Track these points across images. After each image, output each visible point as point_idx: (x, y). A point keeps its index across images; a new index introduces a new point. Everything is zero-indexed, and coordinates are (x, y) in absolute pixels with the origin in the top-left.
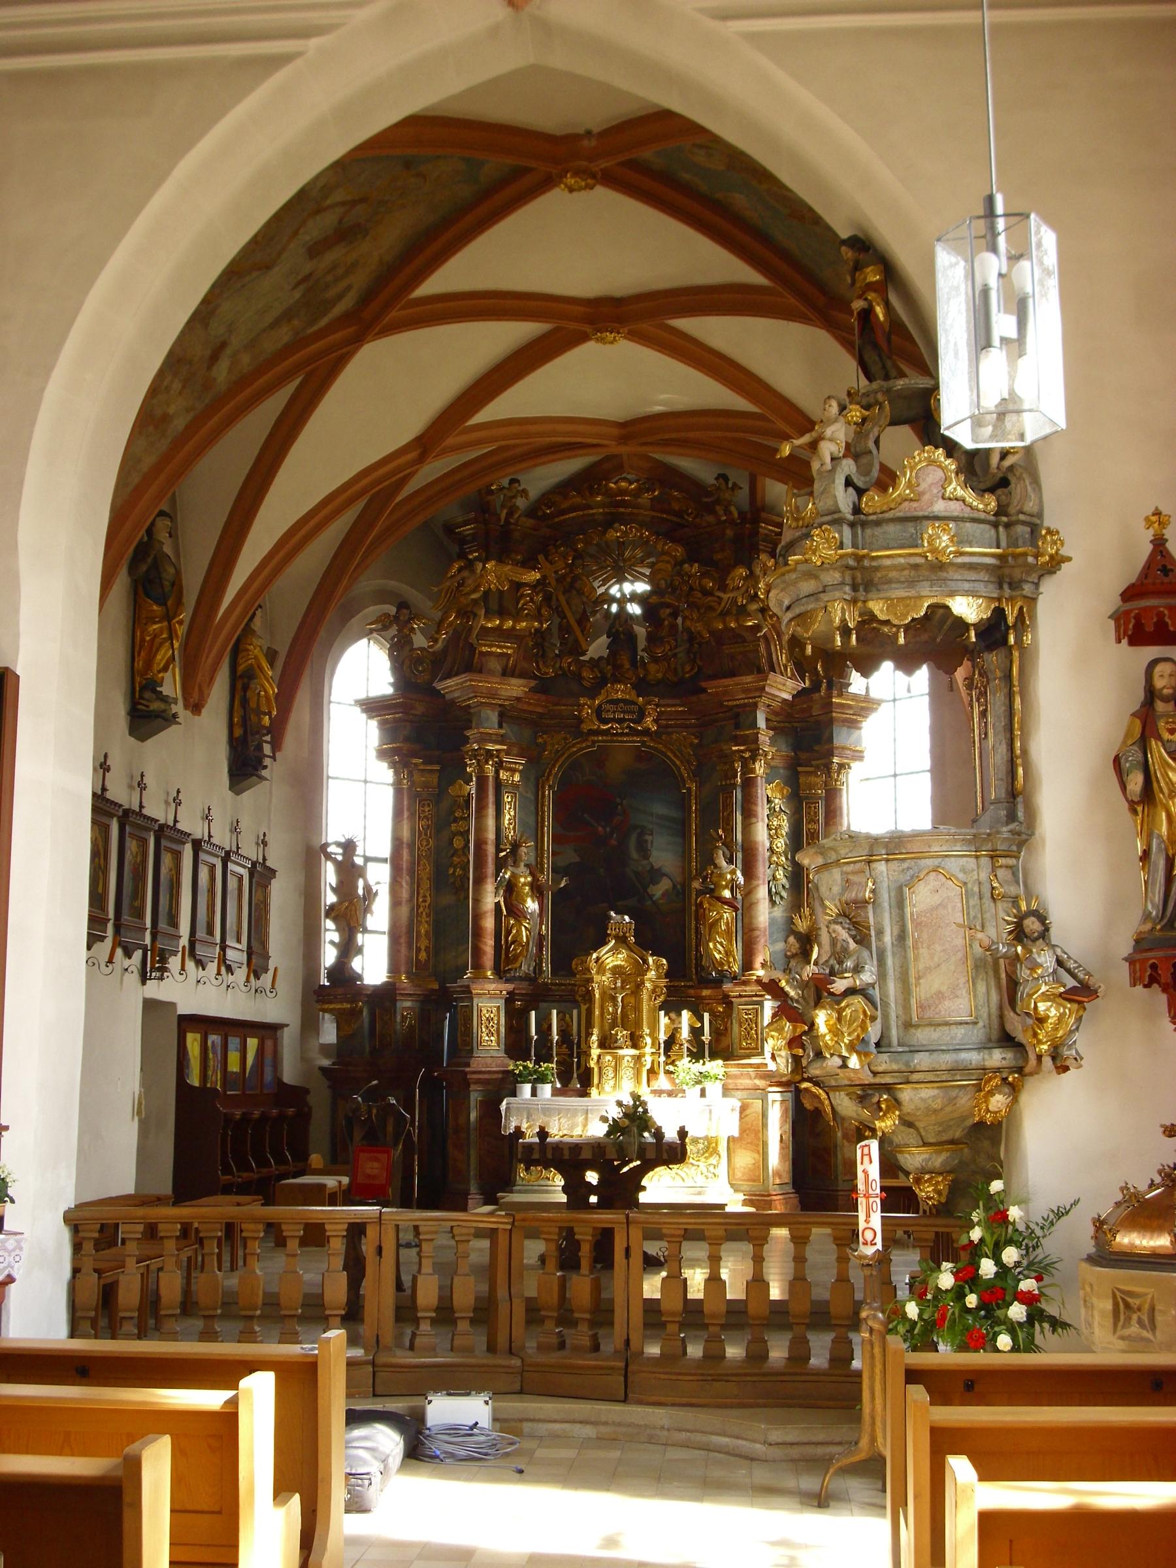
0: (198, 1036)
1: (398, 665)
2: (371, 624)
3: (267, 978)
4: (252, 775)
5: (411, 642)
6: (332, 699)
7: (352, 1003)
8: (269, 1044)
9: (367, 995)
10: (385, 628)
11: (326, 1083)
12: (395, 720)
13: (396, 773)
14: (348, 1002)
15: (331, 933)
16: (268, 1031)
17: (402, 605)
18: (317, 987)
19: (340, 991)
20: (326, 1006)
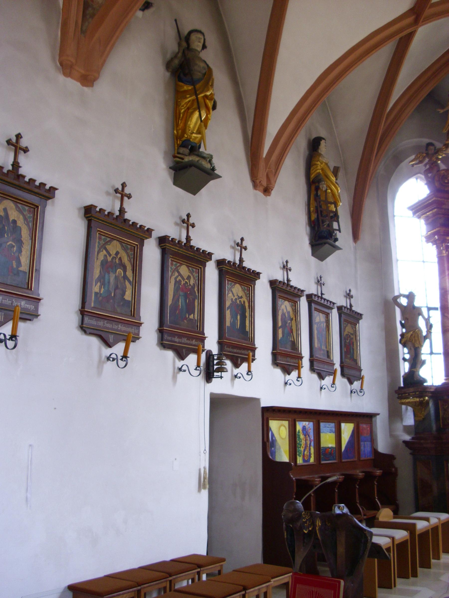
0: (286, 423)
1: (430, 183)
2: (412, 161)
3: (357, 384)
4: (325, 243)
5: (438, 165)
6: (395, 214)
7: (420, 397)
8: (364, 426)
9: (432, 392)
10: (421, 162)
11: (408, 451)
12: (434, 215)
13: (438, 247)
14: (417, 397)
15: (404, 352)
16: (369, 417)
17: (429, 145)
18: (397, 389)
19: (412, 390)
20: (404, 401)
